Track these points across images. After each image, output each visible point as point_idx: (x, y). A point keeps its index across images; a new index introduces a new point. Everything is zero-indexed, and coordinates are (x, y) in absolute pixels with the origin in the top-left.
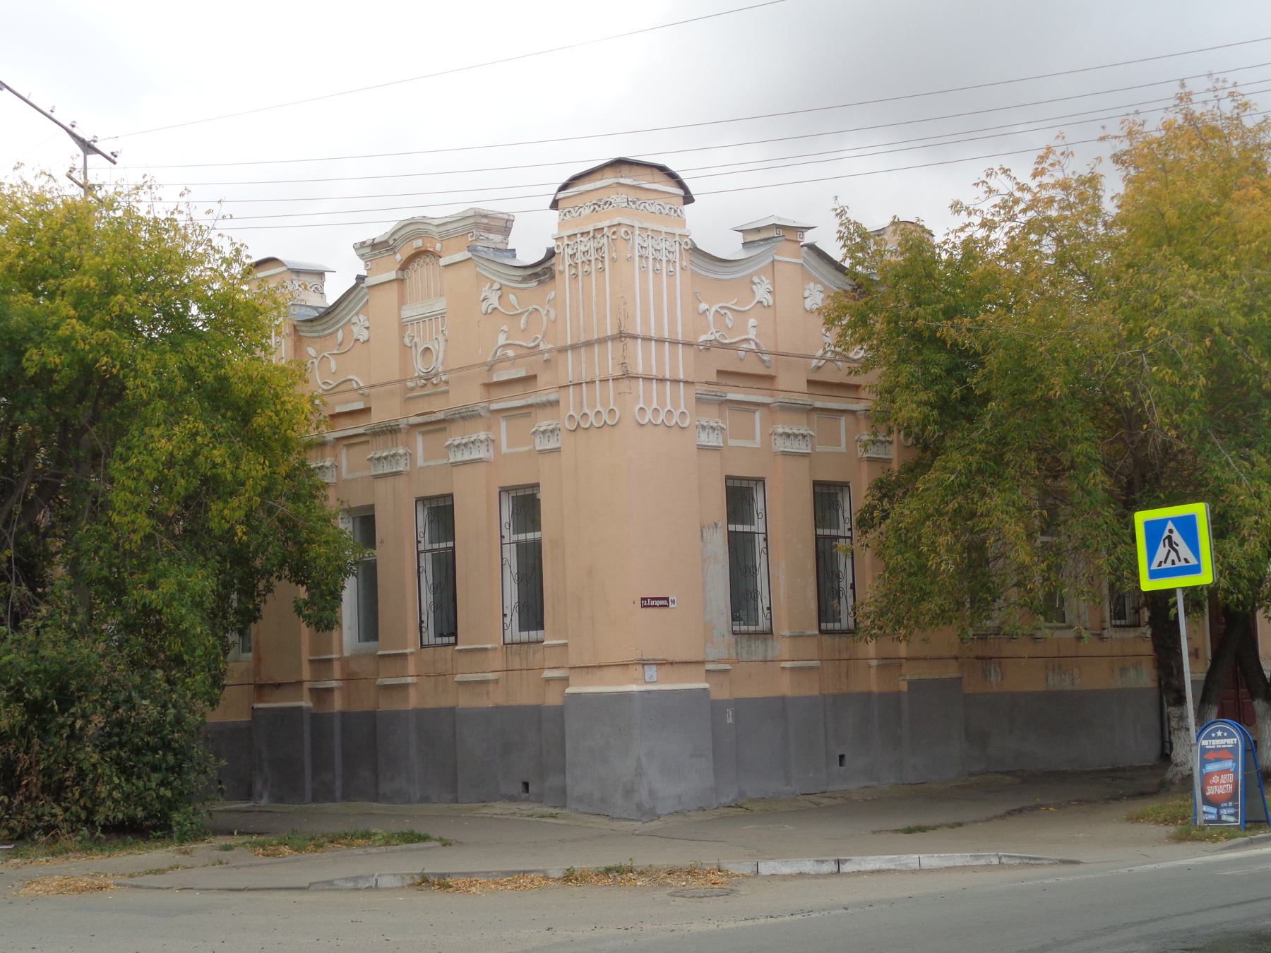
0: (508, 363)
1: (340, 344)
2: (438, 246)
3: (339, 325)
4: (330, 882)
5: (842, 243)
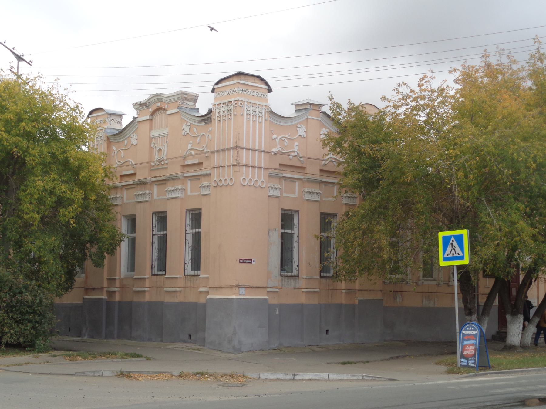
0: (191, 157)
1: (126, 146)
2: (166, 106)
3: (125, 138)
4: (84, 373)
5: (331, 111)
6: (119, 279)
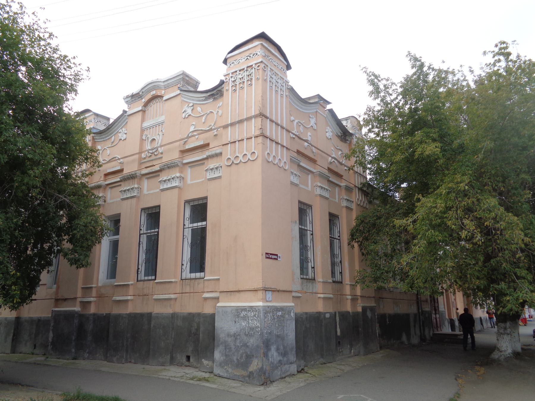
1: (113, 143)
6: (96, 287)
